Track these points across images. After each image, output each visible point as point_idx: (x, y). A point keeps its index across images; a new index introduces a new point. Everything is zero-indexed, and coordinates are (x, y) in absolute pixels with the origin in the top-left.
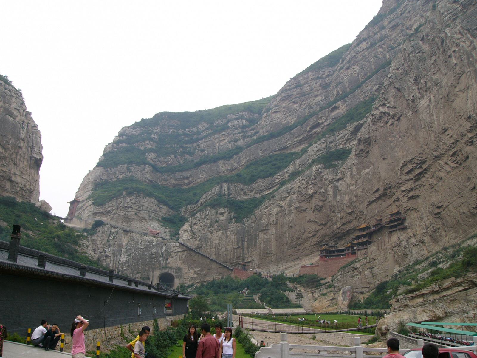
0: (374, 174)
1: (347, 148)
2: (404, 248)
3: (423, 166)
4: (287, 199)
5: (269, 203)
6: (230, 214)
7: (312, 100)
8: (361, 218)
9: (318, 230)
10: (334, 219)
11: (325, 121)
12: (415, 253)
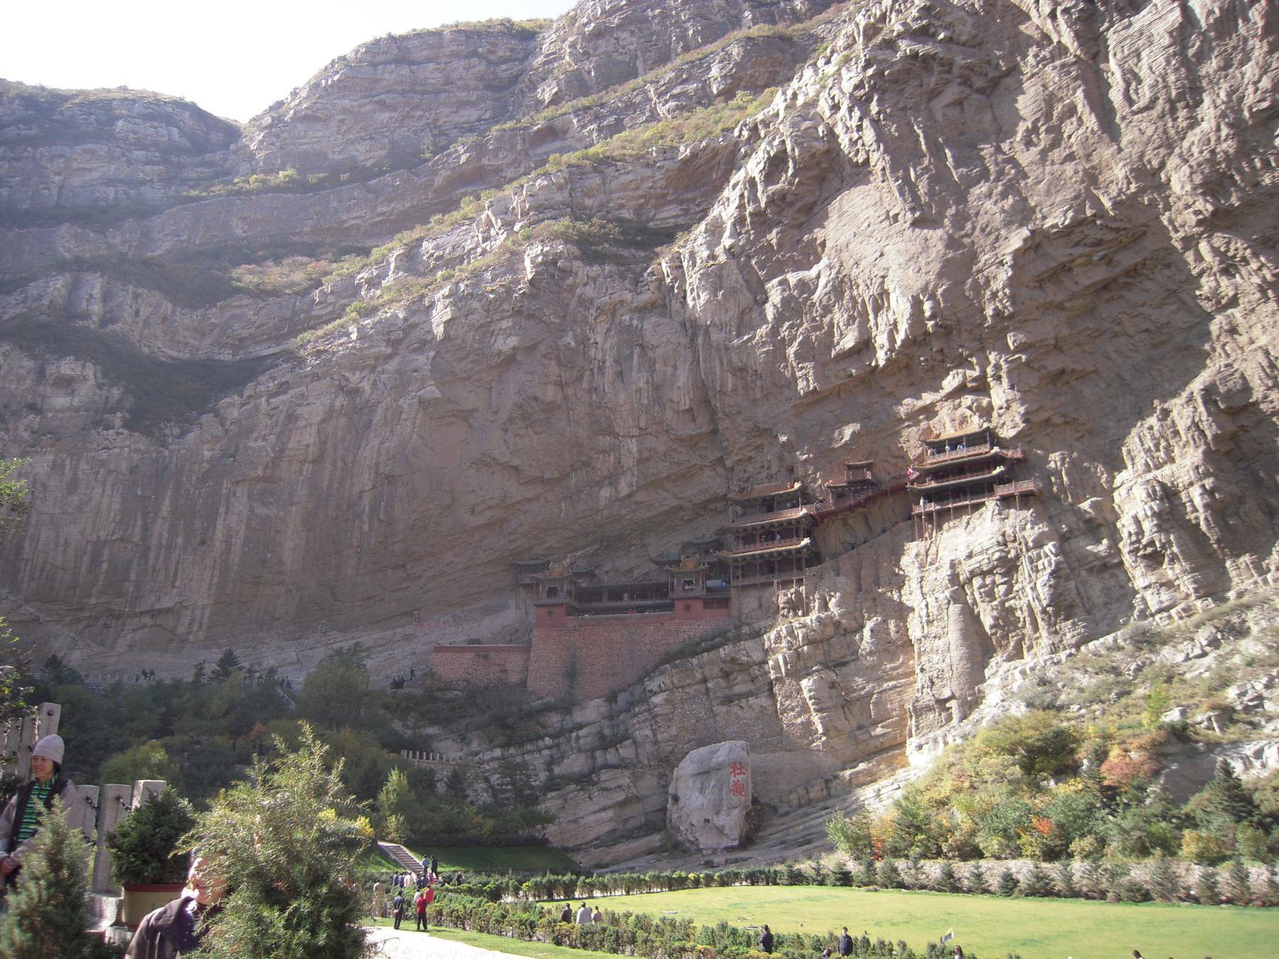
0: (840, 287)
1: (651, 224)
2: (1052, 574)
3: (1119, 257)
4: (386, 367)
5: (297, 370)
6: (104, 392)
7: (446, 111)
8: (751, 458)
9: (519, 503)
10: (604, 464)
11: (509, 165)
12: (1101, 600)
